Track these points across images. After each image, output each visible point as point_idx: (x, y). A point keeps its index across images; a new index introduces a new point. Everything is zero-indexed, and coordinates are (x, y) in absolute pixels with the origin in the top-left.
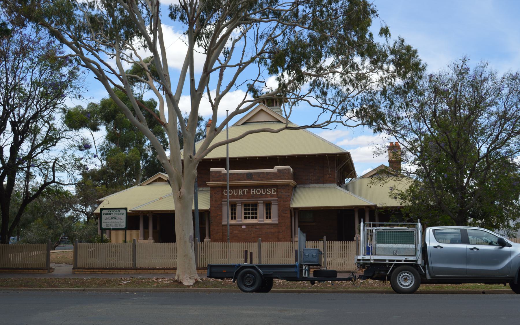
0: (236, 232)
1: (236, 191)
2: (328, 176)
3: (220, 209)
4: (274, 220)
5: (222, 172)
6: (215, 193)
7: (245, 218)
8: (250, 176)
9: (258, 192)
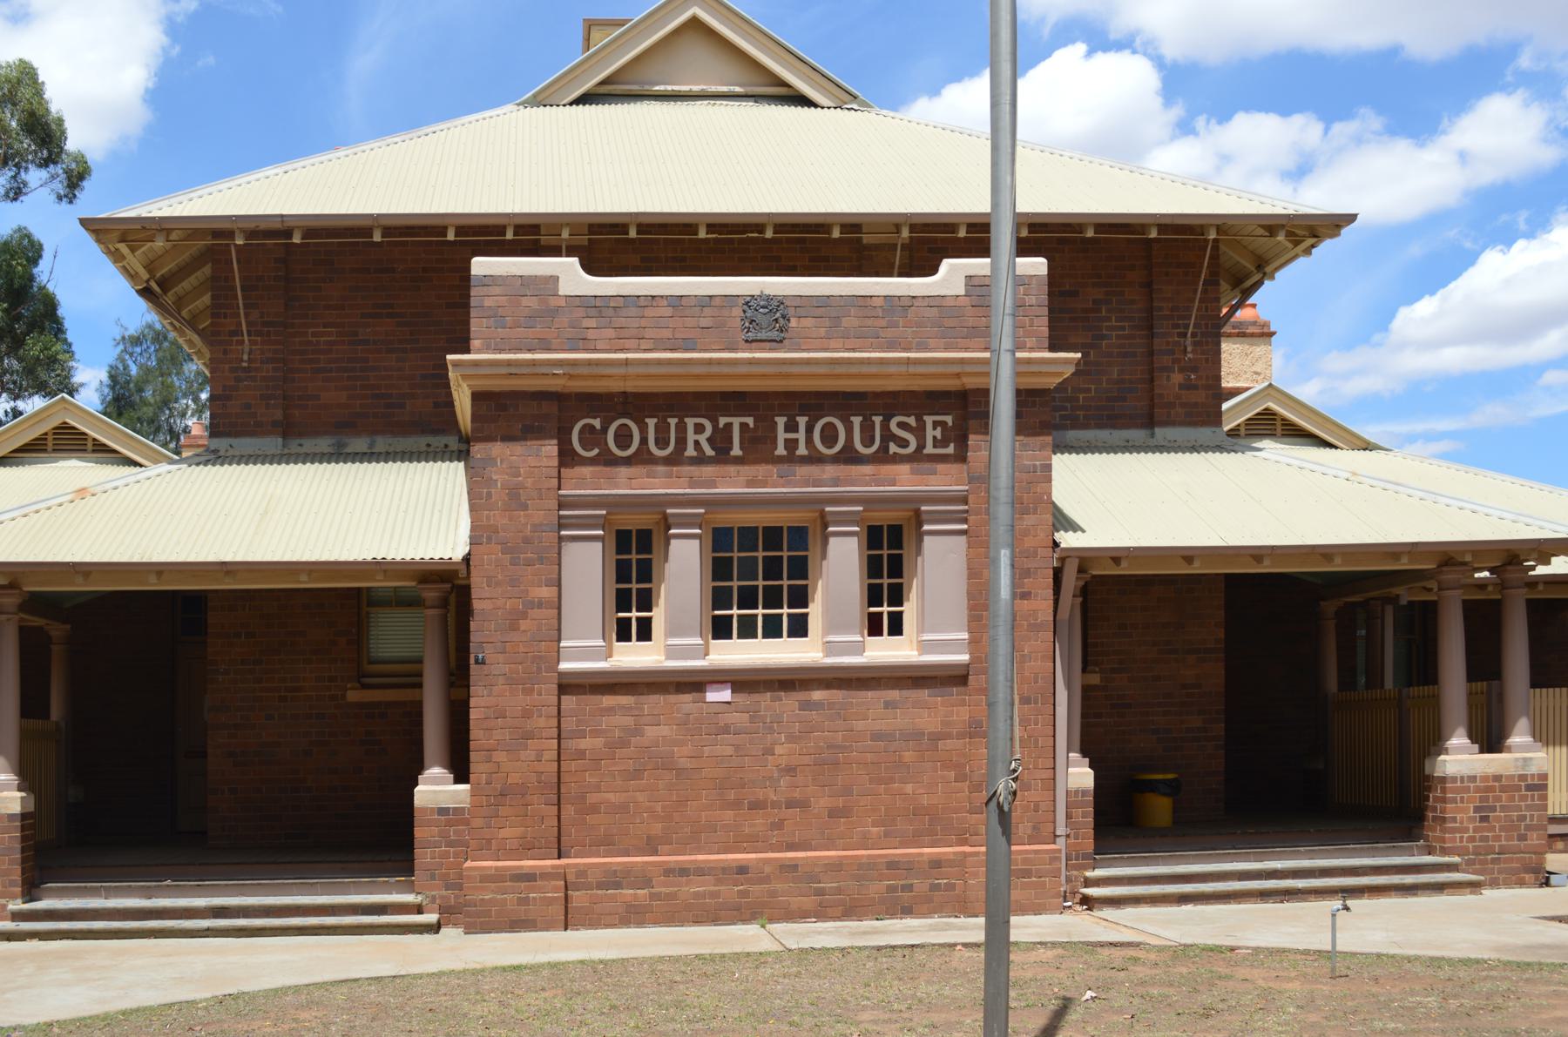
0: (664, 730)
2: (1177, 378)
4: (928, 636)
5: (565, 289)
8: (770, 319)
9: (829, 436)
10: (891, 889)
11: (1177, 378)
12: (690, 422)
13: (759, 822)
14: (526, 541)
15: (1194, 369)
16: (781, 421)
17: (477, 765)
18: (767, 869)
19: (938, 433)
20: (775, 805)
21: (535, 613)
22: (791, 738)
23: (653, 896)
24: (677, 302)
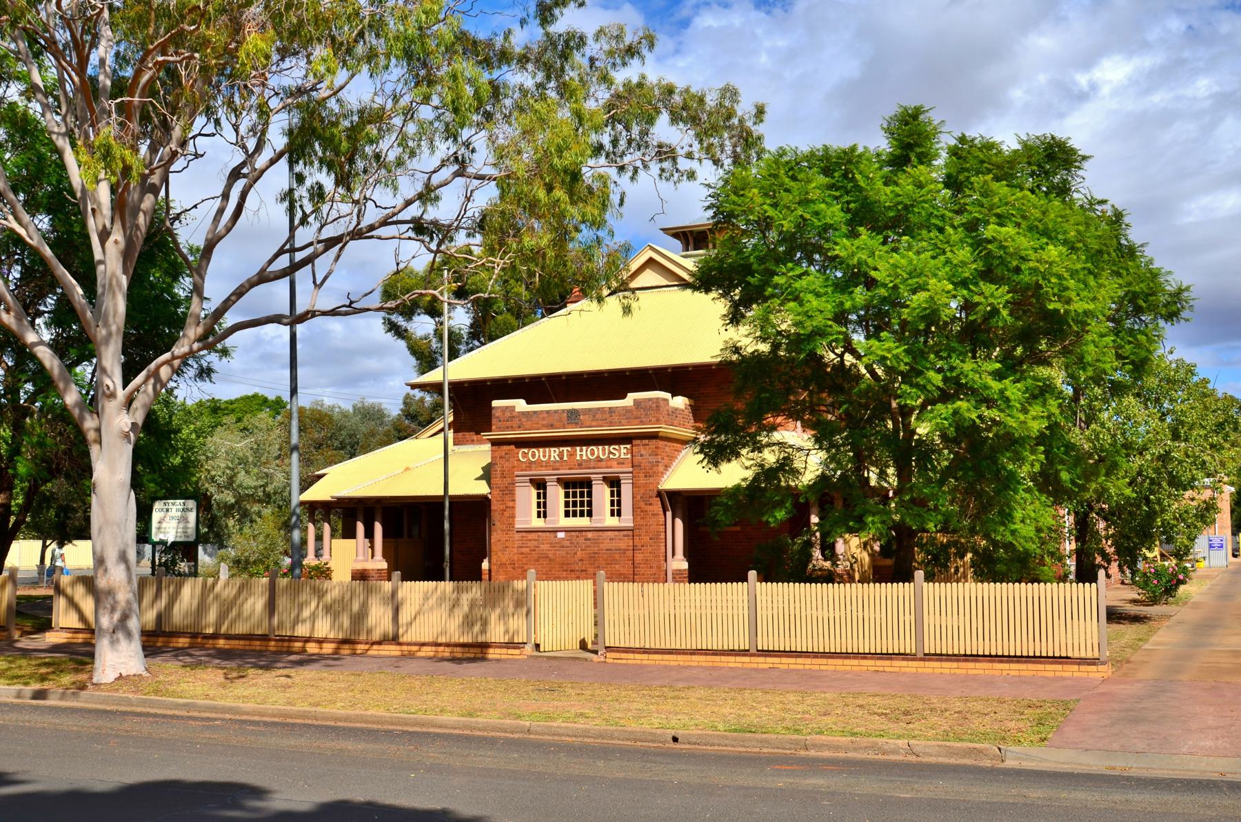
7: (567, 514)
8: (573, 414)
9: (593, 454)
24: (548, 412)
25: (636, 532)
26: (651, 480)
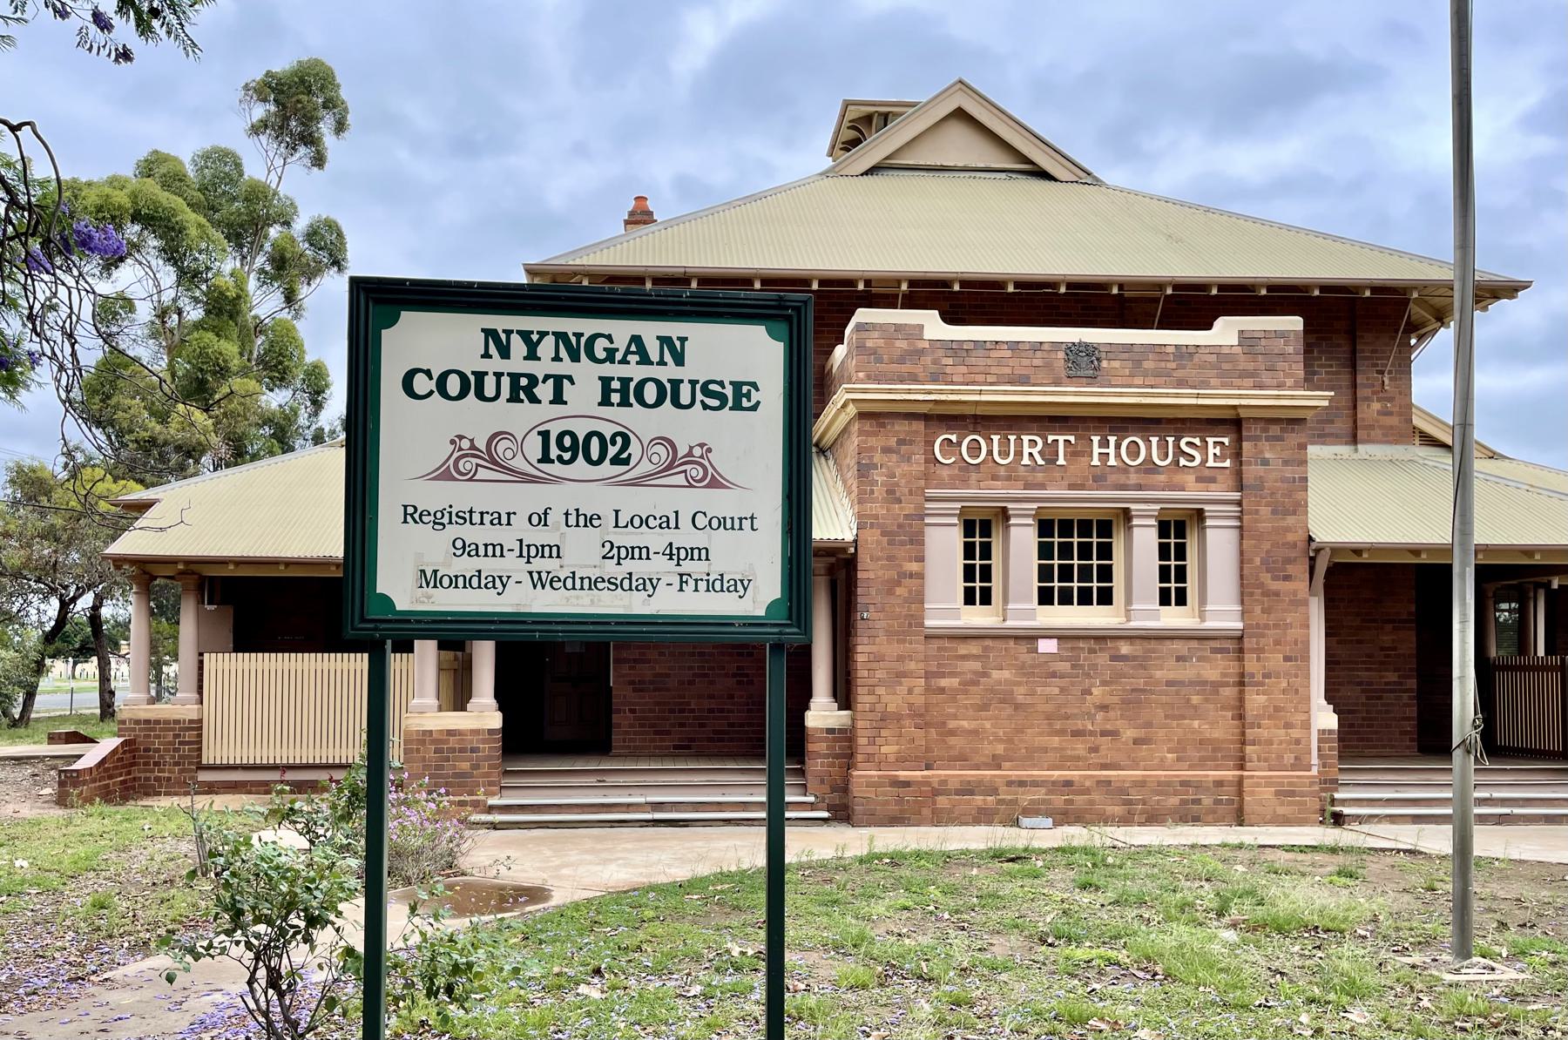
0: (1006, 674)
1: (1005, 442)
2: (1376, 406)
3: (911, 537)
5: (928, 335)
6: (887, 450)
7: (1045, 597)
8: (1083, 361)
9: (1134, 451)
10: (1183, 802)
11: (1376, 406)
12: (1026, 438)
13: (1080, 747)
14: (900, 526)
15: (1391, 399)
16: (1096, 439)
17: (863, 698)
18: (1088, 784)
19: (1217, 451)
20: (1092, 733)
21: (907, 581)
22: (1104, 683)
23: (1000, 802)
24: (1014, 346)
25: (1248, 643)
26: (1291, 520)
